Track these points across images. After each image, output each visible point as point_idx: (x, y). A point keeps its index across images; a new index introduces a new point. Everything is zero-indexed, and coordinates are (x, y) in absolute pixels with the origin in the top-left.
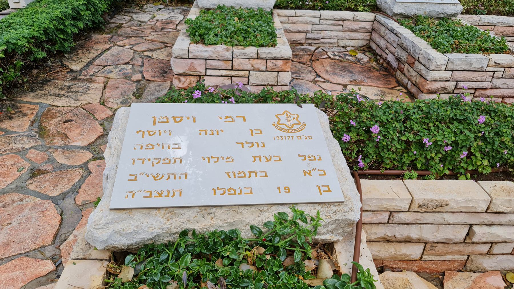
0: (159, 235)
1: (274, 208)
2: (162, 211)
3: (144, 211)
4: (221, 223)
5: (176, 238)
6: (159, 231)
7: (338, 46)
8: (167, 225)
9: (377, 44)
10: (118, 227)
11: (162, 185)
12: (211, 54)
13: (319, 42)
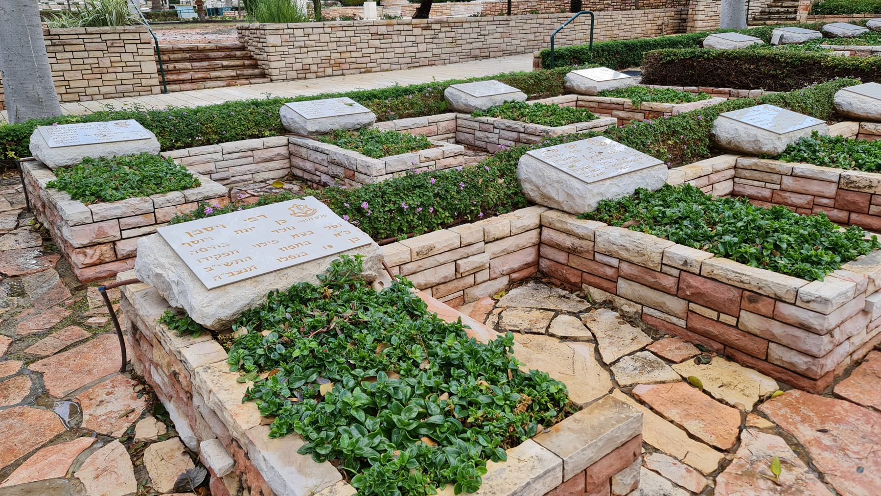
0: (253, 300)
1: (327, 259)
2: (249, 281)
3: (235, 285)
4: (295, 280)
5: (265, 300)
6: (251, 296)
7: (255, 182)
8: (257, 290)
9: (301, 169)
10: (220, 302)
11: (235, 268)
12: (124, 210)
13: (229, 181)
